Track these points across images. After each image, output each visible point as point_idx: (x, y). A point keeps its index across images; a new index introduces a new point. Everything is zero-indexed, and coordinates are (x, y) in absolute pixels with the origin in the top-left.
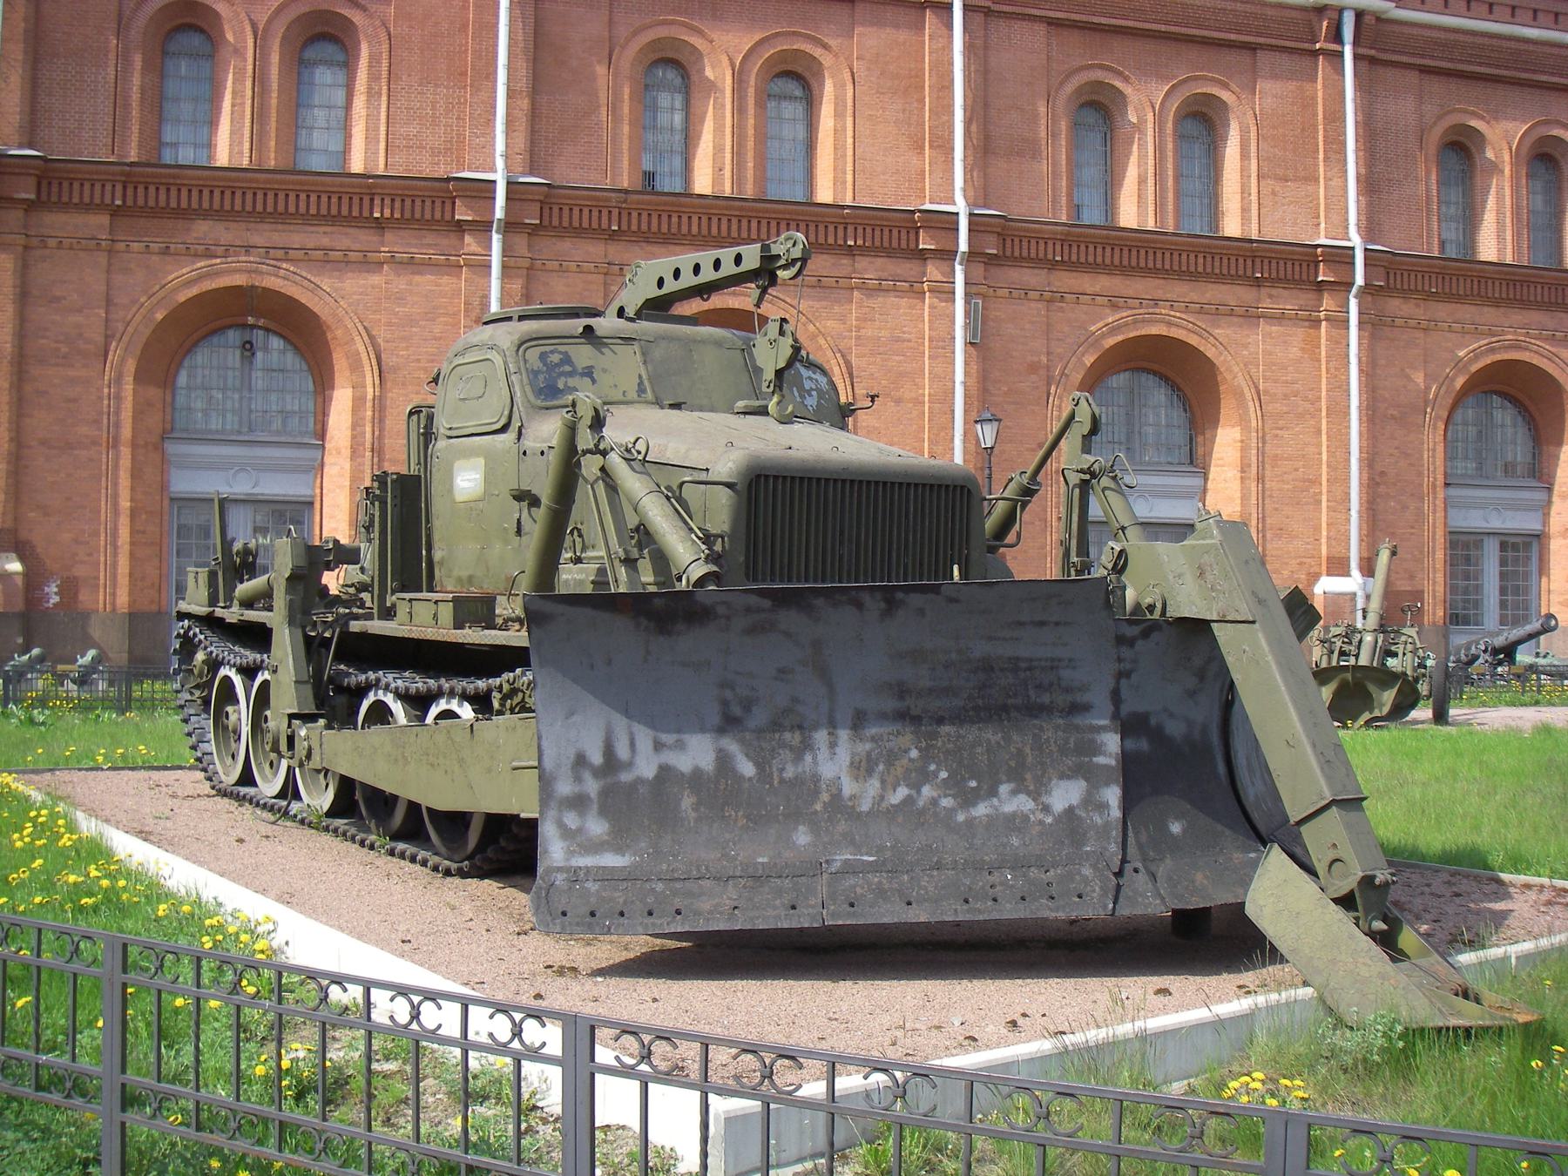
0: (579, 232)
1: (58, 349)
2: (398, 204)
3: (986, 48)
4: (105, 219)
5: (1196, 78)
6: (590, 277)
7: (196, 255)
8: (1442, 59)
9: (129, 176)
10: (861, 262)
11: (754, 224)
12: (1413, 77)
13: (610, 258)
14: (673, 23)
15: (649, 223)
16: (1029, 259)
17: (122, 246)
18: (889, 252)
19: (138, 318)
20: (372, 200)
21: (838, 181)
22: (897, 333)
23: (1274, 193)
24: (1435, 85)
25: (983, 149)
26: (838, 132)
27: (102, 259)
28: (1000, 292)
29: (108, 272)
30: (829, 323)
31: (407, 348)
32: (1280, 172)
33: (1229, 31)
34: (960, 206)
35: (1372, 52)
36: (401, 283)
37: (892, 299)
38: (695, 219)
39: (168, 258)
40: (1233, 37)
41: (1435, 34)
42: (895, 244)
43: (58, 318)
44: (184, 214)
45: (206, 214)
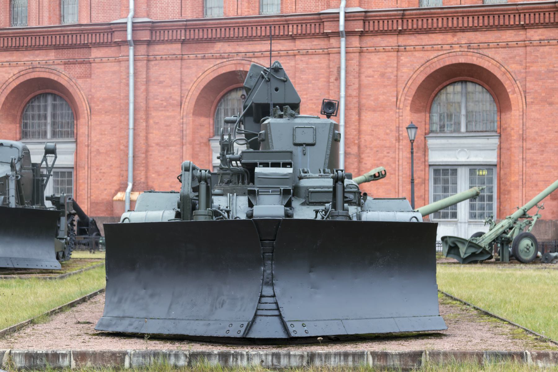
0: (384, 33)
1: (162, 104)
4: (179, 46)
6: (390, 54)
7: (216, 58)
9: (187, 26)
13: (400, 44)
17: (186, 57)
19: (193, 88)
22: (551, 68)
29: (181, 68)
30: (514, 66)
31: (306, 94)
37: (547, 49)
39: (205, 61)
43: (162, 90)
44: (212, 41)
45: (220, 40)
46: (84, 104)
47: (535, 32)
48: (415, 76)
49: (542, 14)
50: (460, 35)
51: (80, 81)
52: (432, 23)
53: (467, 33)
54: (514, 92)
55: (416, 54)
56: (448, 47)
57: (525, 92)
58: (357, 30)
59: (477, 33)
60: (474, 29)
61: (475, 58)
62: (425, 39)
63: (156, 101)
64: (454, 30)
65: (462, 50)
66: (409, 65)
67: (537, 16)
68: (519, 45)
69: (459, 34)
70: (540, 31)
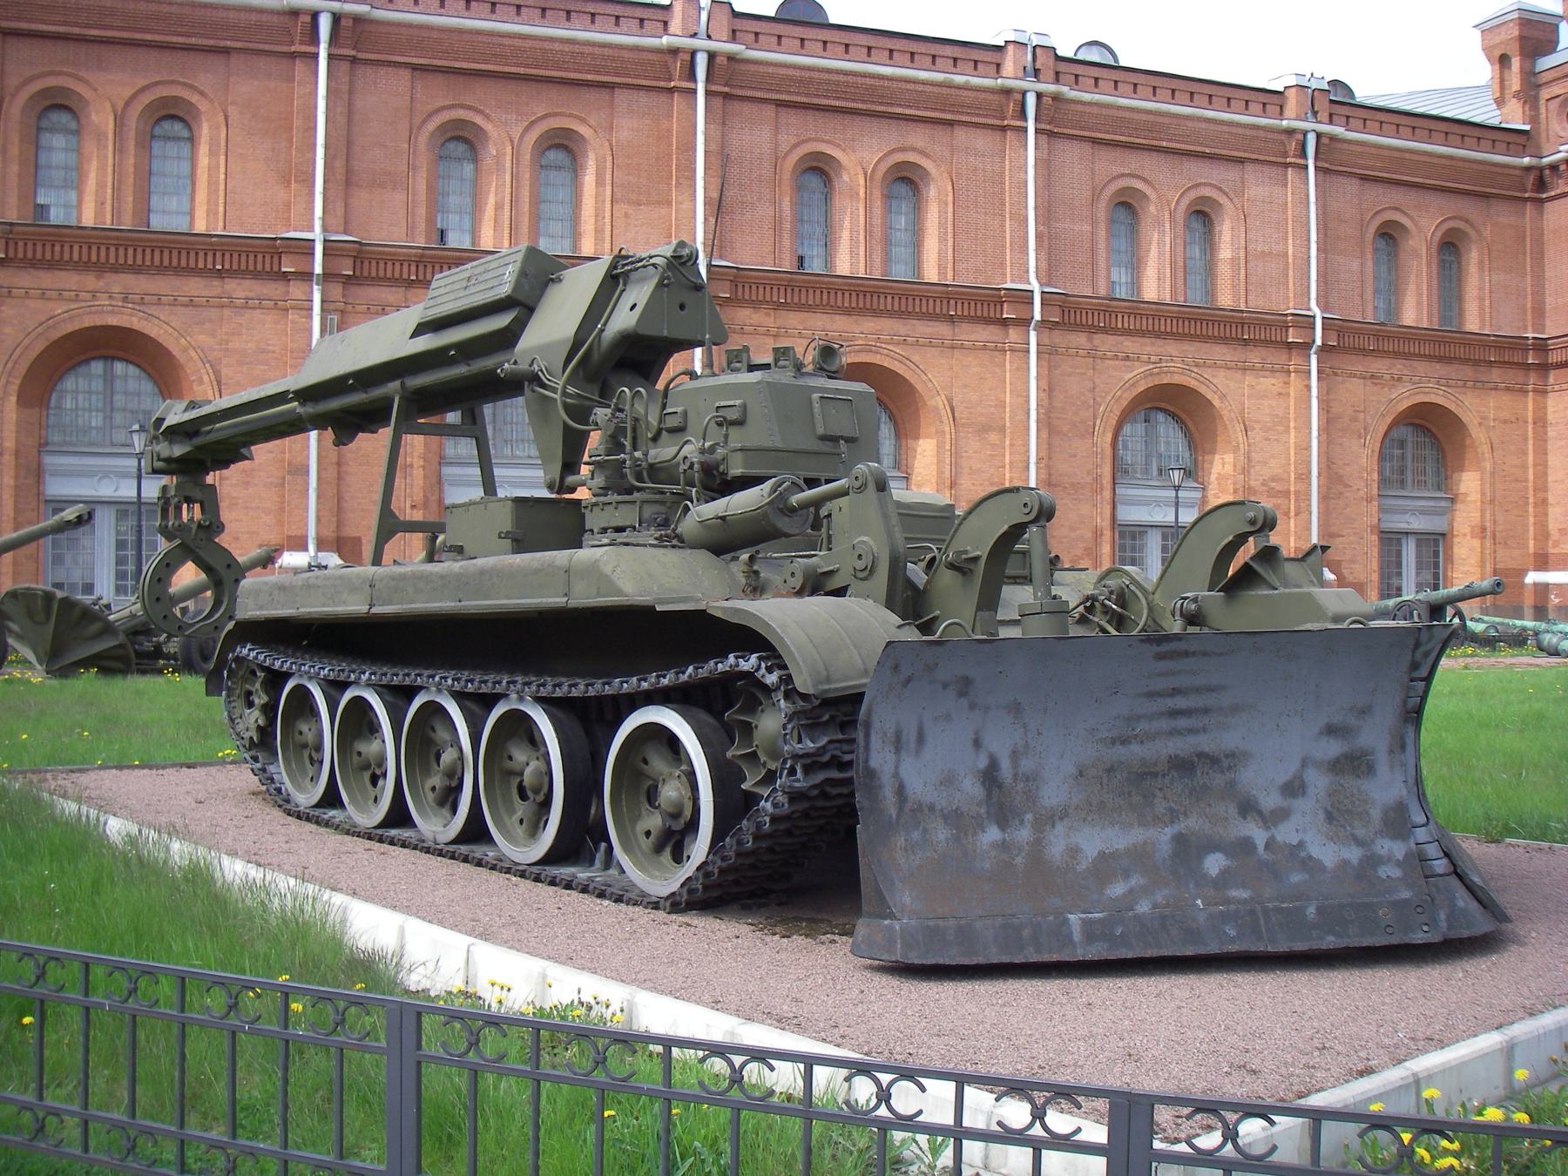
3: (351, 92)
5: (556, 115)
8: (798, 94)
11: (131, 251)
12: (770, 111)
14: (60, 73)
15: (34, 251)
16: (385, 279)
18: (256, 275)
21: (211, 213)
23: (626, 215)
24: (791, 118)
25: (345, 179)
26: (212, 170)
28: (359, 308)
30: (201, 337)
32: (634, 197)
33: (588, 72)
34: (317, 234)
35: (726, 89)
37: (257, 314)
38: (76, 247)
40: (589, 77)
41: (790, 72)
42: (259, 267)
48: (26, 342)
49: (251, 257)
50: (110, 277)
52: (62, 252)
54: (201, 382)
55: (27, 302)
56: (89, 296)
57: (219, 383)
59: (141, 277)
60: (136, 270)
61: (135, 320)
62: (47, 279)
64: (101, 268)
67: (243, 257)
70: (247, 283)
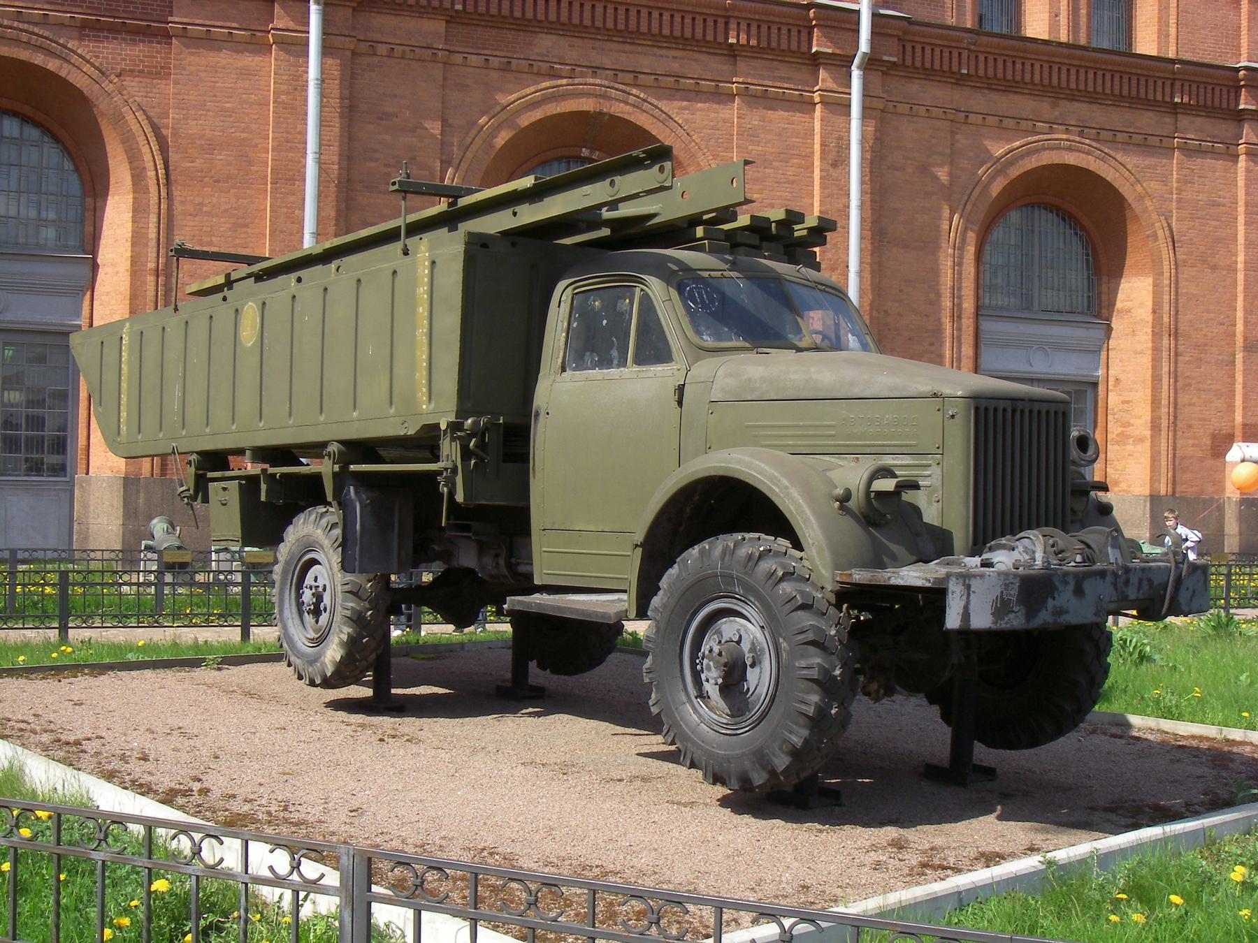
2: (754, 30)
4: (439, 26)
6: (939, 124)
7: (538, 74)
10: (1184, 121)
17: (458, 58)
19: (478, 141)
20: (727, 23)
21: (1162, 35)
27: (437, 71)
30: (1152, 184)
36: (755, 118)
43: (388, 138)
46: (145, 150)
47: (1191, 122)
50: (1065, 105)
51: (131, 83)
53: (1077, 104)
58: (885, 58)
59: (1095, 107)
63: (372, 164)
65: (1072, 138)
66: (971, 154)
68: (1133, 141)
69: (1062, 103)
